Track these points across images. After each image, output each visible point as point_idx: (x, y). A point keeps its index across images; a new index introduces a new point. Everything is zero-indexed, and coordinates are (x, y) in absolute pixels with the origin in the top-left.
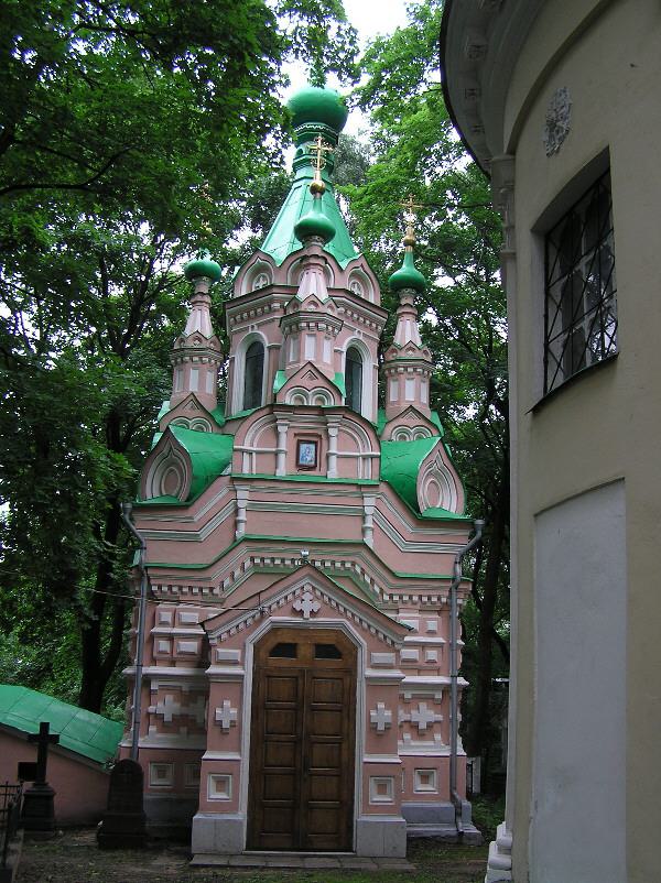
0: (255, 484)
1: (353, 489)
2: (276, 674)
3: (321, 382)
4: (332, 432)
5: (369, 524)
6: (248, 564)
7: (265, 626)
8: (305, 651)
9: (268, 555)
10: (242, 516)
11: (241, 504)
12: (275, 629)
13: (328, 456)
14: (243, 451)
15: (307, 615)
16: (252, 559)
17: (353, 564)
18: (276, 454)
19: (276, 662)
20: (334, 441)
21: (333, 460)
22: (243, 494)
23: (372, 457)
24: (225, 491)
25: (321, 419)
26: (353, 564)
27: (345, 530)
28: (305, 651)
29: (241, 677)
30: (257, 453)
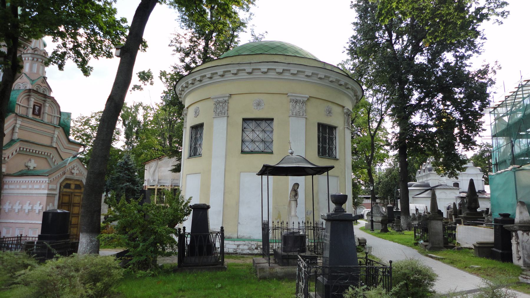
0: (24, 119)
1: (53, 127)
2: (65, 194)
3: (46, 86)
4: (47, 105)
5: (55, 139)
6: (18, 150)
7: (64, 177)
8: (73, 186)
9: (26, 146)
10: (17, 130)
11: (18, 126)
12: (66, 179)
13: (43, 113)
14: (18, 104)
15: (75, 174)
16: (20, 148)
17: (50, 154)
18: (27, 108)
19: (65, 190)
20: (47, 108)
21: (46, 116)
22: (19, 122)
23: (57, 117)
24: (12, 120)
25: (43, 99)
26: (50, 154)
27: (46, 141)
28: (73, 186)
29: (56, 194)
30: (23, 106)
